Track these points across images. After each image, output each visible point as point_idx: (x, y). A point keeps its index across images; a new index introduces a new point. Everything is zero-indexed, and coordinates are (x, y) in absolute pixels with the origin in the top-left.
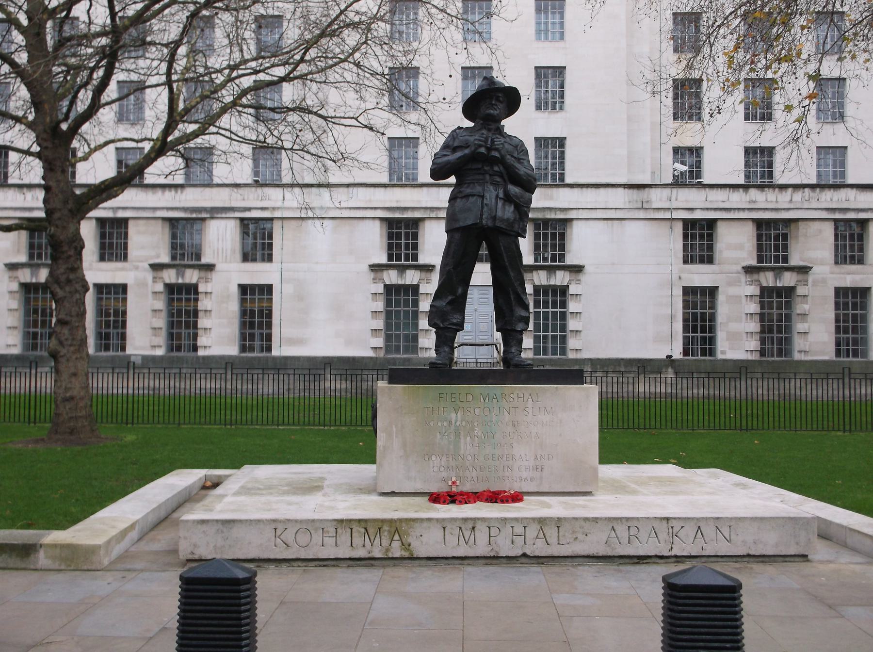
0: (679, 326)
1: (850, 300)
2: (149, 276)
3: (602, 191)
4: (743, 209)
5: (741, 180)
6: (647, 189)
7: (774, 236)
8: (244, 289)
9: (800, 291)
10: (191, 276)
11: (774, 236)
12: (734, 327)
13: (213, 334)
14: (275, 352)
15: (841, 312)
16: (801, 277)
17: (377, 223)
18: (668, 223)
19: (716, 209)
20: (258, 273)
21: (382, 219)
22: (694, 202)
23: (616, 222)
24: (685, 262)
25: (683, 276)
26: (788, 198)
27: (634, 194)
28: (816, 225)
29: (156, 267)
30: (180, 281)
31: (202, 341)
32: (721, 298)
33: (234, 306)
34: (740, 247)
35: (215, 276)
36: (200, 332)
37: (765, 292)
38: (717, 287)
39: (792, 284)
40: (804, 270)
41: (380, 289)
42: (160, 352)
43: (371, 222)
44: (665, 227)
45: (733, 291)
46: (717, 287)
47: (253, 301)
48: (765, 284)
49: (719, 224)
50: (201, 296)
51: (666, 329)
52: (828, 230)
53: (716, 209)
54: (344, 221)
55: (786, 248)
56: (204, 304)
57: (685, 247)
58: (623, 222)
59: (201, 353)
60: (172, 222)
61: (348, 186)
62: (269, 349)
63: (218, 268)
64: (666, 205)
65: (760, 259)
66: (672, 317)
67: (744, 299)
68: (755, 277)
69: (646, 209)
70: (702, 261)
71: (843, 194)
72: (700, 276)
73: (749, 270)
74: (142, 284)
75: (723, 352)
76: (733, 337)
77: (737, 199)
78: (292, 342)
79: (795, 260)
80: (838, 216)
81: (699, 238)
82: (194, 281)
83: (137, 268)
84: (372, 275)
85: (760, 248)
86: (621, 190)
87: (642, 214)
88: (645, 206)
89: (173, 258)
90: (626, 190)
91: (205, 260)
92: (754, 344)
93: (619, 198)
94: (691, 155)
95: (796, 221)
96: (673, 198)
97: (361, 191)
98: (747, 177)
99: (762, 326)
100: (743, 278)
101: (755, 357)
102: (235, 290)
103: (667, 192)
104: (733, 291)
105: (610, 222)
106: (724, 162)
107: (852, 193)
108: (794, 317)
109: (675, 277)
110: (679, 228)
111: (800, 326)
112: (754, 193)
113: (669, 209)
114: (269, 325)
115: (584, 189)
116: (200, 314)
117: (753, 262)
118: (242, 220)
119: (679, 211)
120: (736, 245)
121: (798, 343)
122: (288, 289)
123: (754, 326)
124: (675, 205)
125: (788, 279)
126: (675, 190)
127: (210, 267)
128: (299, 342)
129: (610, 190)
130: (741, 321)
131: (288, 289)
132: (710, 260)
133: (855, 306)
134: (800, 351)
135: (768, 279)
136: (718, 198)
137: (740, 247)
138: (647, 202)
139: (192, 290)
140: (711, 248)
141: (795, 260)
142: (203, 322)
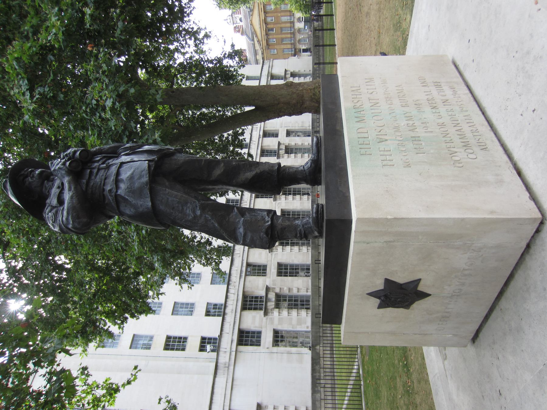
0: (294, 350)
1: (283, 271)
3: (215, 391)
4: (235, 315)
5: (221, 318)
6: (219, 364)
7: (250, 303)
9: (278, 290)
11: (250, 303)
12: (294, 322)
15: (288, 274)
16: (271, 290)
18: (238, 353)
19: (234, 329)
22: (229, 340)
23: (235, 383)
24: (259, 345)
25: (267, 346)
26: (233, 295)
27: (220, 372)
28: (247, 283)
32: (279, 328)
34: (254, 318)
37: (277, 306)
38: (274, 330)
39: (274, 294)
40: (268, 289)
44: (241, 356)
45: (276, 321)
46: (274, 330)
48: (274, 306)
49: (241, 327)
51: (295, 356)
52: (250, 278)
53: (234, 329)
55: (256, 297)
57: (251, 345)
58: (235, 378)
64: (228, 354)
65: (261, 309)
66: (289, 353)
67: (280, 317)
68: (269, 311)
69: (229, 365)
70: (260, 337)
71: (233, 272)
72: (267, 338)
73: (266, 314)
75: (308, 327)
76: (300, 322)
77: (229, 318)
79: (263, 293)
80: (244, 274)
81: (247, 338)
85: (255, 309)
86: (217, 379)
87: (232, 368)
88: (227, 366)
90: (217, 376)
92: (303, 313)
93: (221, 380)
94: (204, 342)
95: (244, 292)
96: (225, 350)
98: (219, 315)
99: (294, 308)
100: (270, 316)
101: (310, 312)
103: (221, 354)
104: (276, 321)
105: (234, 386)
106: (211, 327)
107: (234, 268)
108: (291, 294)
109: (267, 351)
110: (241, 348)
111: (295, 292)
112: (228, 310)
113: (230, 353)
115: (213, 401)
117: (262, 312)
119: (232, 347)
120: (253, 320)
121: (303, 292)
123: (294, 312)
124: (228, 350)
125: (272, 296)
126: (221, 349)
129: (216, 386)
130: (292, 318)
132: (260, 333)
133: (286, 269)
134: (307, 291)
135: (271, 305)
136: (228, 327)
137: (254, 318)
138: (225, 364)
140: (253, 332)
141: (263, 293)
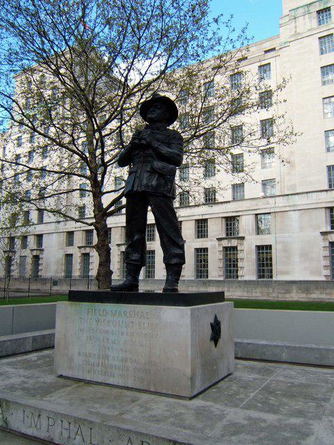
2: (217, 243)
8: (259, 247)
10: (234, 243)
13: (245, 270)
14: (274, 279)
17: (324, 210)
20: (264, 240)
21: (326, 208)
29: (219, 239)
30: (229, 245)
31: (240, 273)
33: (254, 256)
35: (245, 242)
36: (239, 269)
41: (327, 244)
42: (222, 279)
43: (321, 210)
47: (263, 253)
50: (239, 252)
54: (306, 211)
56: (240, 256)
59: (239, 279)
60: (227, 218)
61: (307, 193)
62: (271, 277)
63: (246, 238)
74: (214, 247)
78: (282, 273)
82: (235, 245)
83: (212, 240)
84: (322, 237)
89: (227, 235)
91: (240, 235)
97: (314, 194)
102: (254, 248)
114: (271, 265)
116: (239, 260)
118: (257, 215)
122: (279, 247)
127: (243, 238)
128: (287, 273)
131: (279, 247)
139: (235, 248)
142: (240, 264)
